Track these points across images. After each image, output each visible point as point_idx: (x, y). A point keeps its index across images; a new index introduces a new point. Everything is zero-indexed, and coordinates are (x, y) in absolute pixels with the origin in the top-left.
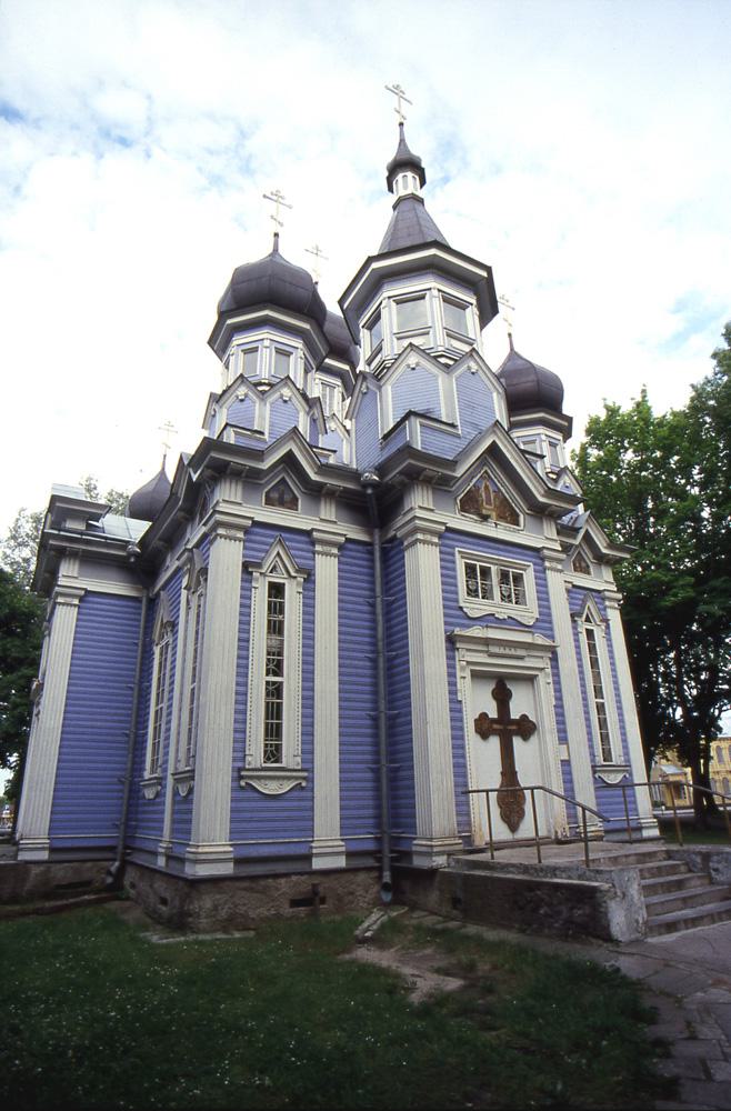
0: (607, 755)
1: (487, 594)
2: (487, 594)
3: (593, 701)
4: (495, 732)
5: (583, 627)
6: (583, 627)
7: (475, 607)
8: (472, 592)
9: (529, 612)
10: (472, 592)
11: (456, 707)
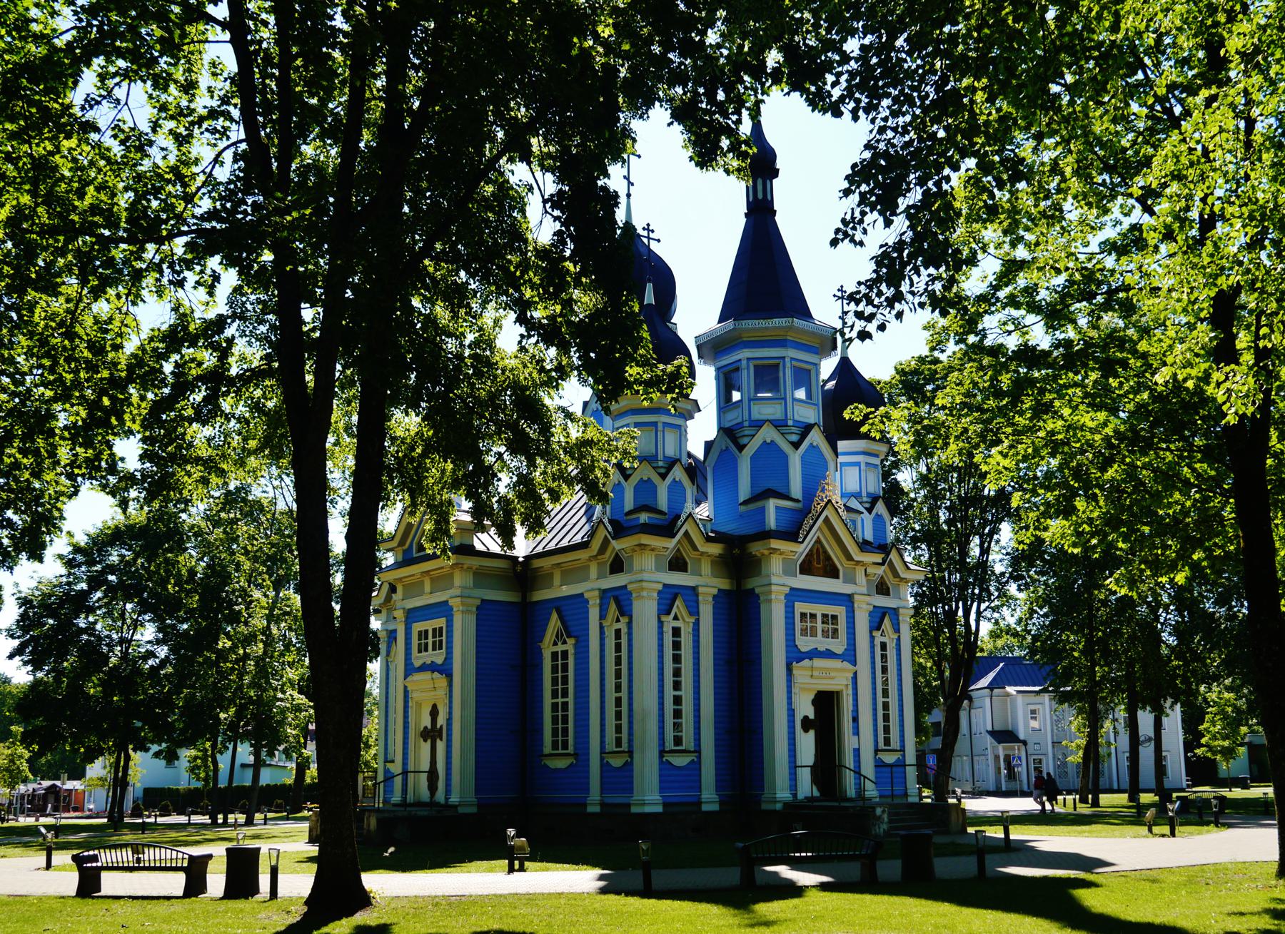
0: (887, 741)
1: (814, 634)
2: (814, 634)
3: (880, 700)
7: (804, 644)
8: (804, 632)
9: (838, 646)
11: (791, 713)
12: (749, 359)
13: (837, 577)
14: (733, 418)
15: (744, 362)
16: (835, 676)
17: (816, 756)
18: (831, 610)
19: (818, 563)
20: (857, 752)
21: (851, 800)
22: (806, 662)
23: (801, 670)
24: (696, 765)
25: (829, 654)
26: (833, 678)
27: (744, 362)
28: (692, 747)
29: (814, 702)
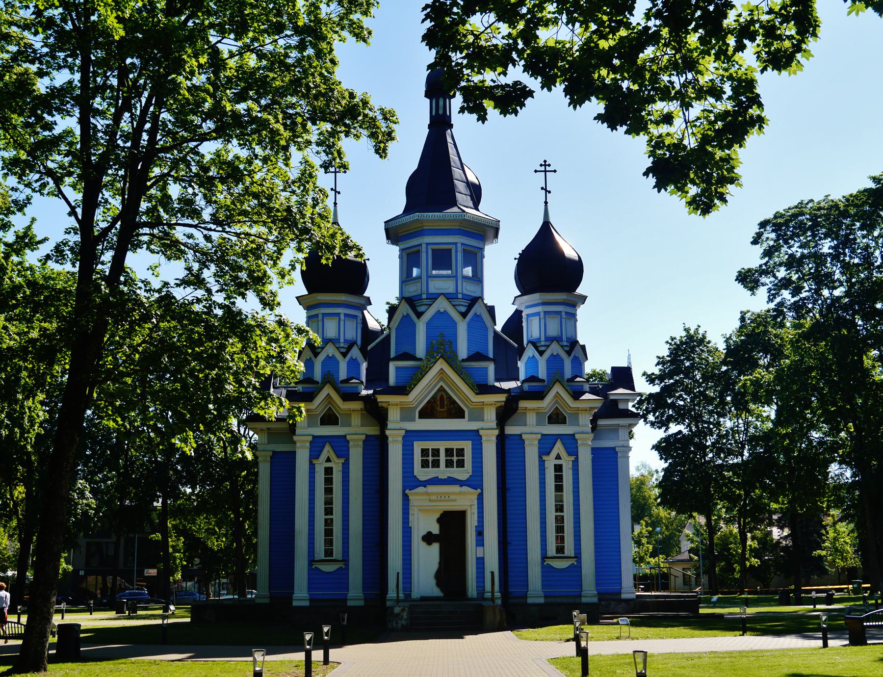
1: (436, 464)
2: (436, 464)
4: (436, 541)
5: (550, 462)
6: (550, 462)
10: (425, 464)
12: (427, 244)
13: (463, 417)
14: (412, 290)
15: (424, 246)
16: (462, 500)
17: (440, 563)
18: (455, 445)
19: (442, 406)
20: (481, 562)
21: (472, 599)
22: (421, 489)
23: (417, 497)
24: (344, 572)
25: (451, 481)
26: (455, 500)
27: (424, 246)
28: (340, 557)
29: (439, 521)
